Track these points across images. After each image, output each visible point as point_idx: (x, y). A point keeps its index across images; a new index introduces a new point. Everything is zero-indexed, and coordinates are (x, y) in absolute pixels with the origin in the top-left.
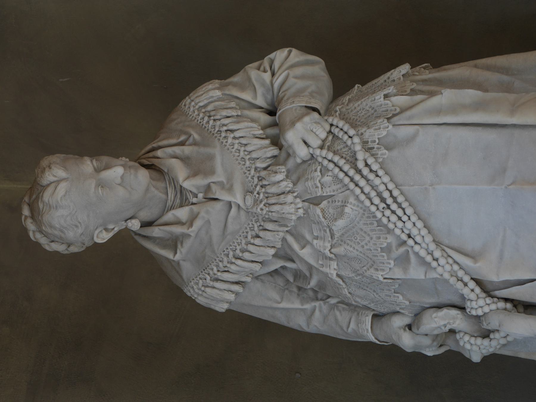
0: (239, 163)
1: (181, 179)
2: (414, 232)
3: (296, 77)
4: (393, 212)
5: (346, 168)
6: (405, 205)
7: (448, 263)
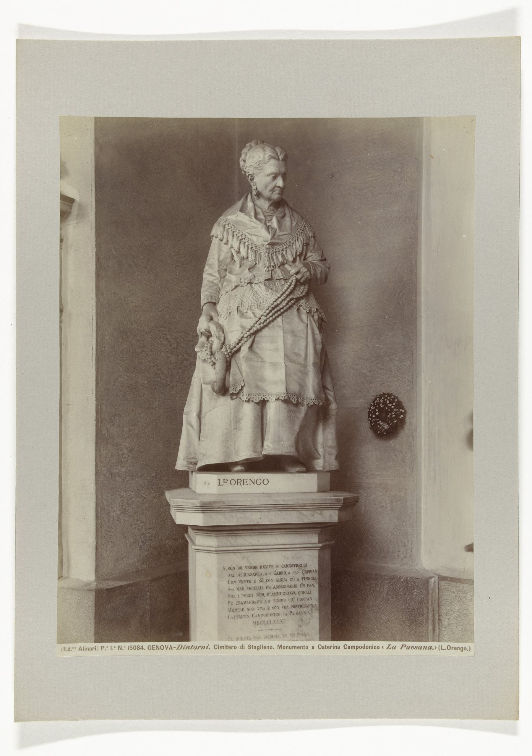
5: (289, 290)
6: (274, 317)
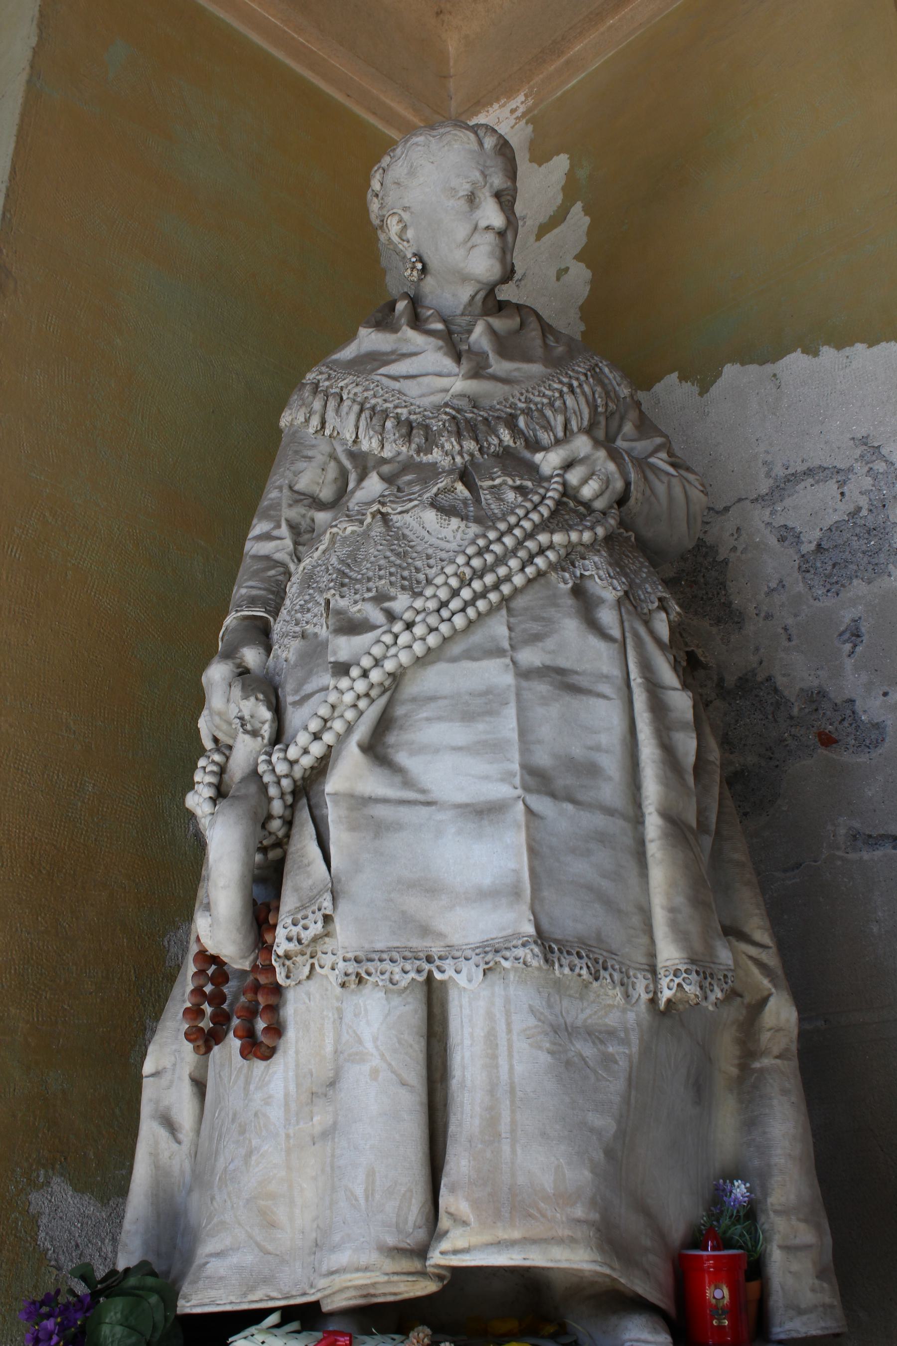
0: (522, 394)
1: (490, 320)
2: (419, 630)
3: (669, 487)
4: (455, 593)
7: (359, 697)
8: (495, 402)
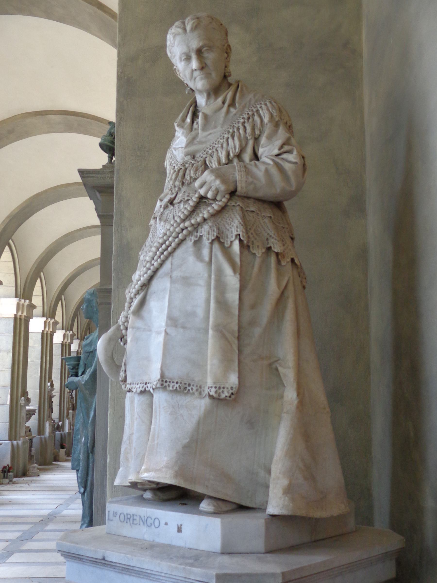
0: (210, 146)
3: (267, 171)
8: (201, 153)
